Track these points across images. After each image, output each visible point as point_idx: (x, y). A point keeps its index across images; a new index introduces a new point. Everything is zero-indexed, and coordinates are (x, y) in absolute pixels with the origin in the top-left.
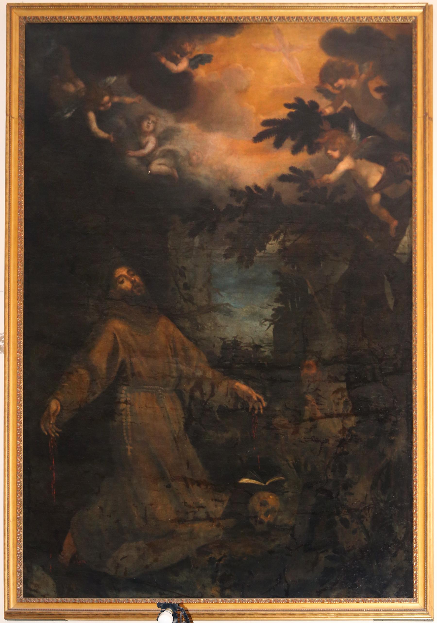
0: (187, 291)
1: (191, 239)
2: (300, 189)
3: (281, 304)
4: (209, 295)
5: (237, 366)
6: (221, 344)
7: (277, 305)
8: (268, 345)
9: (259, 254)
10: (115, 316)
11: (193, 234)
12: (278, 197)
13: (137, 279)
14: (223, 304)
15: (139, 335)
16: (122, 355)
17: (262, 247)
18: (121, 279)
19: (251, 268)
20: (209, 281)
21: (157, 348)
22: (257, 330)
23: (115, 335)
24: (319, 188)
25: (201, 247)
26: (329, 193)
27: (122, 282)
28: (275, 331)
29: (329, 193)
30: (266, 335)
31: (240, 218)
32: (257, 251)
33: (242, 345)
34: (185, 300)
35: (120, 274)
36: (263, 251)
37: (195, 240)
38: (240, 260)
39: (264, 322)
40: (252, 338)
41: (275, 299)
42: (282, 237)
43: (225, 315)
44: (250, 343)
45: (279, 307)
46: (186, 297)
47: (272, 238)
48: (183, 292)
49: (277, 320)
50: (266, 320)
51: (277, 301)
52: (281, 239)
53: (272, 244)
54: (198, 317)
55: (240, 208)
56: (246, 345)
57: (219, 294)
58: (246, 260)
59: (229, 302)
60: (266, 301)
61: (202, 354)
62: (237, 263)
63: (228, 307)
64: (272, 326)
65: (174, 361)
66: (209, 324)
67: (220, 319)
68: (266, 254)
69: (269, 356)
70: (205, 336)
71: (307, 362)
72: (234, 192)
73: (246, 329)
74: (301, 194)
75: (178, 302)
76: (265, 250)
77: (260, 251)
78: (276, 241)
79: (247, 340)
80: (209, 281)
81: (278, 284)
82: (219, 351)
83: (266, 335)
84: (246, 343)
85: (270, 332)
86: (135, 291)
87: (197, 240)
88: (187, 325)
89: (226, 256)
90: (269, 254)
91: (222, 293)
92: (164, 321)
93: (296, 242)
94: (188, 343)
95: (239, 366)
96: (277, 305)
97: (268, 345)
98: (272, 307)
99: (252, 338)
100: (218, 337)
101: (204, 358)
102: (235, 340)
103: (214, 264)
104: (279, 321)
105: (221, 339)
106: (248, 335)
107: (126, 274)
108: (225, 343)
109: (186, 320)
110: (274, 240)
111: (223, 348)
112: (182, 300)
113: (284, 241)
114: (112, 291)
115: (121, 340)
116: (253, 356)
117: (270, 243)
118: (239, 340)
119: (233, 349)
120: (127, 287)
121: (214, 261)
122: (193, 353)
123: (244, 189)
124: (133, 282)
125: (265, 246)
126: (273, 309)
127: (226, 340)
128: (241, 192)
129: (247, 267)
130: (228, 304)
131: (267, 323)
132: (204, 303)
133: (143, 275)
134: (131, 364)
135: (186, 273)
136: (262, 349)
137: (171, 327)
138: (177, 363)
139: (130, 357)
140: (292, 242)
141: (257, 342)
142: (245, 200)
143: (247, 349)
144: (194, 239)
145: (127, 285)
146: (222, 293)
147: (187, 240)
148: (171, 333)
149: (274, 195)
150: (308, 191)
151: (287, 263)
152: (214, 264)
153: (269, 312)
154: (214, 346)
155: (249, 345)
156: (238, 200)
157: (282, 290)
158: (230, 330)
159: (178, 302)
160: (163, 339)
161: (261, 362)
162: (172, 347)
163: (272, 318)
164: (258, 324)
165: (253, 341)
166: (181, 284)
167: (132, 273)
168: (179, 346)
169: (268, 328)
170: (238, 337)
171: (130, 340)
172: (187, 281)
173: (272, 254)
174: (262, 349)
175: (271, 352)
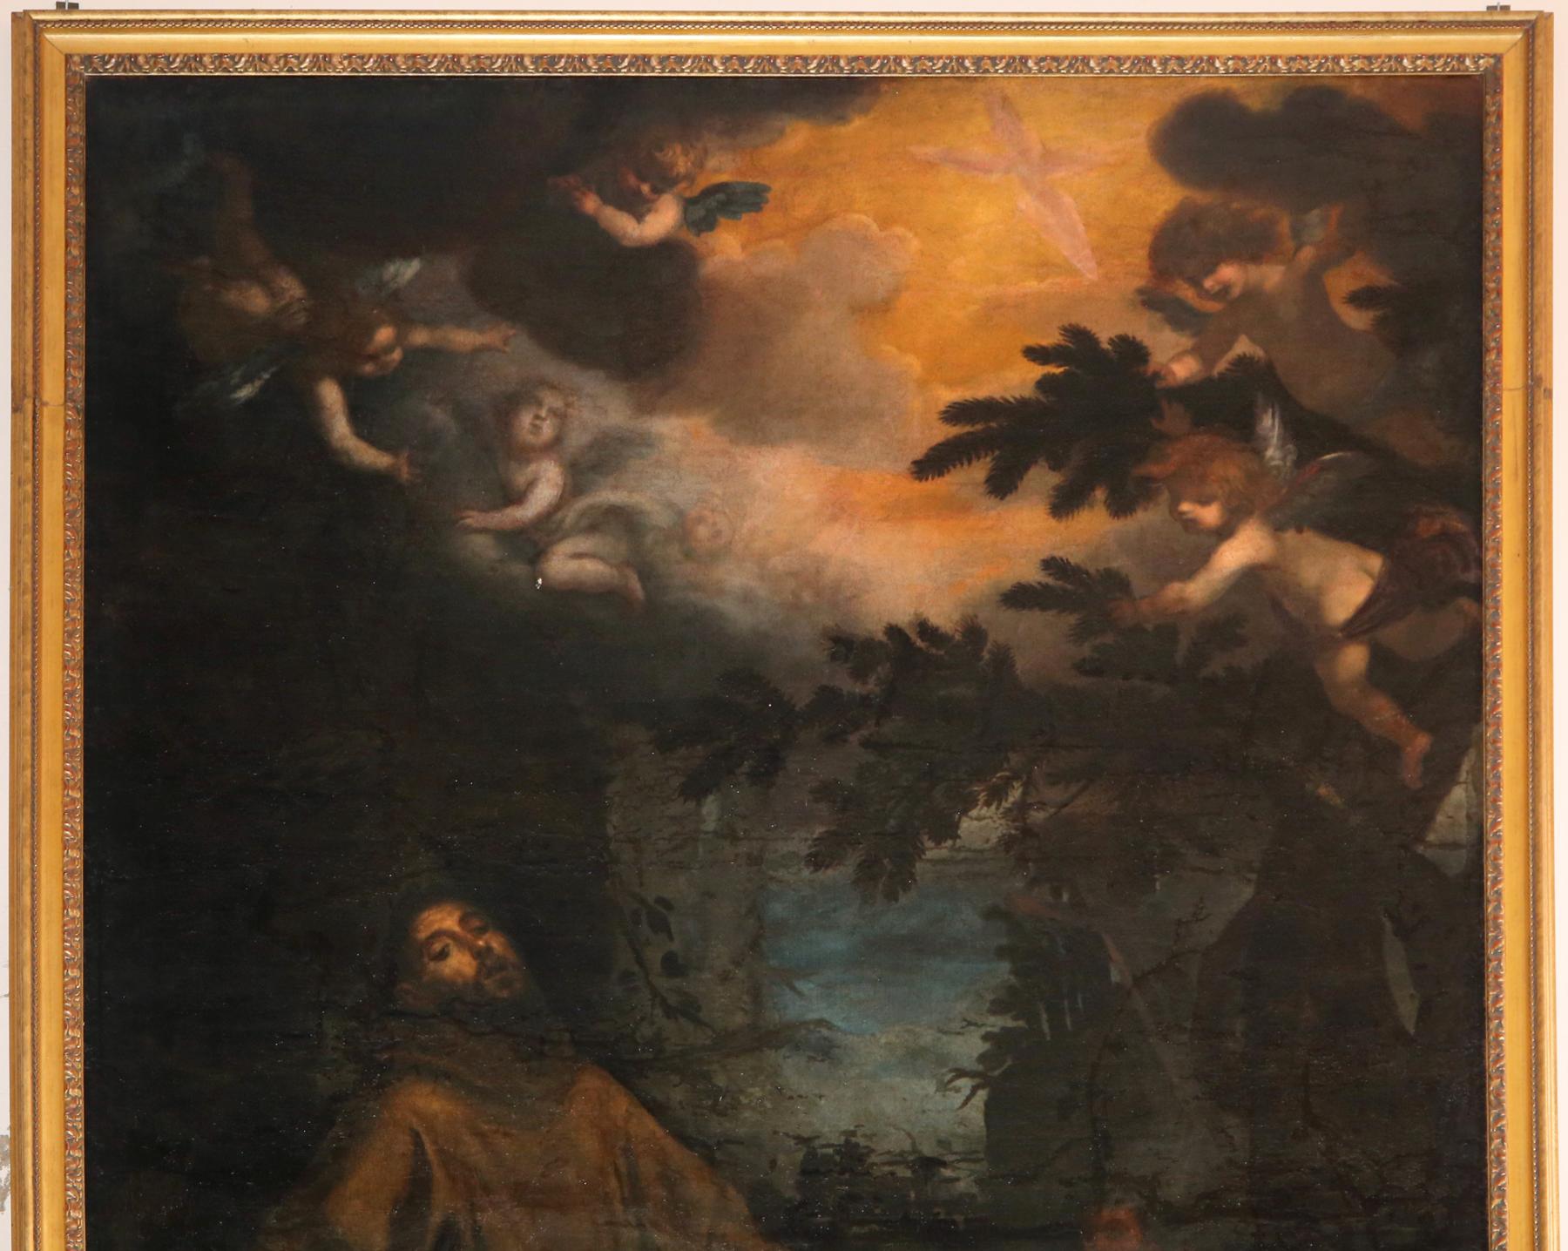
0: (677, 982)
1: (691, 805)
2: (1080, 633)
3: (1015, 1018)
4: (756, 995)
5: (855, 1229)
6: (800, 1156)
7: (997, 1023)
8: (968, 1157)
9: (933, 852)
10: (417, 1070)
11: (695, 789)
12: (1003, 659)
13: (495, 942)
14: (805, 1024)
15: (506, 1134)
16: (443, 1205)
17: (946, 829)
18: (437, 947)
19: (903, 900)
20: (754, 945)
21: (569, 1175)
22: (929, 1106)
23: (417, 1135)
24: (1149, 627)
25: (728, 834)
26: (1184, 643)
27: (443, 955)
28: (990, 1108)
29: (1184, 643)
30: (961, 1123)
31: (865, 732)
32: (929, 844)
33: (873, 1159)
34: (670, 1012)
35: (436, 927)
36: (949, 843)
37: (704, 811)
38: (867, 873)
39: (950, 1081)
40: (909, 1135)
41: (993, 1002)
42: (1015, 794)
43: (811, 1058)
44: (902, 1153)
45: (1003, 1028)
46: (673, 1000)
47: (982, 797)
48: (663, 983)
49: (996, 1073)
50: (961, 1073)
51: (998, 1007)
52: (1011, 799)
53: (979, 819)
54: (715, 1067)
55: (865, 700)
56: (885, 1158)
57: (793, 988)
58: (888, 869)
59: (826, 1015)
60: (961, 1007)
61: (732, 1192)
62: (856, 882)
63: (825, 1032)
64: (982, 1094)
65: (631, 1219)
66: (756, 1091)
67: (793, 1071)
68: (959, 850)
69: (973, 1196)
70: (741, 1131)
71: (1106, 1213)
72: (846, 646)
73: (889, 1107)
74: (1086, 650)
75: (643, 1019)
76: (956, 837)
77: (938, 842)
78: (993, 807)
79: (894, 1142)
80: (754, 945)
81: (1001, 953)
82: (791, 1182)
83: (961, 1123)
84: (889, 1152)
85: (975, 1114)
86: (489, 984)
87: (710, 807)
88: (677, 1095)
89: (817, 861)
90: (969, 850)
91: (801, 985)
92: (592, 1082)
93: (1065, 811)
94: (681, 1158)
95: (865, 1230)
96: (997, 1023)
97: (968, 1157)
98: (983, 1031)
99: (909, 1135)
100: (787, 1135)
101: (739, 1205)
102: (847, 1142)
103: (774, 887)
104: (1008, 1078)
105: (800, 1140)
106: (894, 1126)
107: (457, 929)
108: (811, 1154)
109: (675, 1079)
110: (988, 804)
111: (804, 1172)
112: (658, 1011)
113: (1022, 807)
114: (405, 986)
115: (440, 1151)
116: (913, 1195)
117: (974, 813)
118: (862, 1142)
119: (842, 1173)
120: (458, 972)
121: (772, 878)
122: (700, 1190)
123: (881, 637)
124: (480, 955)
125: (957, 826)
126: (985, 1038)
127: (817, 1143)
128: (869, 644)
129: (891, 896)
130: (821, 1022)
131: (965, 1084)
132: (739, 1019)
133: (515, 930)
134: (476, 1230)
135: (673, 920)
136: (947, 1173)
137: (621, 1105)
138: (640, 1225)
139: (473, 1209)
140: (1052, 810)
141: (928, 1150)
142: (883, 670)
143: (893, 1174)
144: (699, 805)
145: (459, 963)
146: (801, 985)
147: (676, 808)
148: (620, 1123)
149: (986, 655)
150: (1109, 639)
151: (1033, 882)
152: (774, 887)
153: (969, 1048)
154: (773, 1163)
155: (899, 1159)
156: (859, 674)
157: (1015, 972)
158: (829, 1109)
159: (643, 1019)
160: (589, 1145)
161: (942, 1217)
162: (623, 1170)
163: (981, 1068)
164: (930, 1087)
165: (914, 1144)
166: (654, 956)
167: (476, 923)
168: (648, 1167)
169: (968, 1099)
170: (859, 1133)
171: (472, 1149)
172: (675, 946)
173: (982, 851)
174: (947, 1173)
175: (979, 1182)
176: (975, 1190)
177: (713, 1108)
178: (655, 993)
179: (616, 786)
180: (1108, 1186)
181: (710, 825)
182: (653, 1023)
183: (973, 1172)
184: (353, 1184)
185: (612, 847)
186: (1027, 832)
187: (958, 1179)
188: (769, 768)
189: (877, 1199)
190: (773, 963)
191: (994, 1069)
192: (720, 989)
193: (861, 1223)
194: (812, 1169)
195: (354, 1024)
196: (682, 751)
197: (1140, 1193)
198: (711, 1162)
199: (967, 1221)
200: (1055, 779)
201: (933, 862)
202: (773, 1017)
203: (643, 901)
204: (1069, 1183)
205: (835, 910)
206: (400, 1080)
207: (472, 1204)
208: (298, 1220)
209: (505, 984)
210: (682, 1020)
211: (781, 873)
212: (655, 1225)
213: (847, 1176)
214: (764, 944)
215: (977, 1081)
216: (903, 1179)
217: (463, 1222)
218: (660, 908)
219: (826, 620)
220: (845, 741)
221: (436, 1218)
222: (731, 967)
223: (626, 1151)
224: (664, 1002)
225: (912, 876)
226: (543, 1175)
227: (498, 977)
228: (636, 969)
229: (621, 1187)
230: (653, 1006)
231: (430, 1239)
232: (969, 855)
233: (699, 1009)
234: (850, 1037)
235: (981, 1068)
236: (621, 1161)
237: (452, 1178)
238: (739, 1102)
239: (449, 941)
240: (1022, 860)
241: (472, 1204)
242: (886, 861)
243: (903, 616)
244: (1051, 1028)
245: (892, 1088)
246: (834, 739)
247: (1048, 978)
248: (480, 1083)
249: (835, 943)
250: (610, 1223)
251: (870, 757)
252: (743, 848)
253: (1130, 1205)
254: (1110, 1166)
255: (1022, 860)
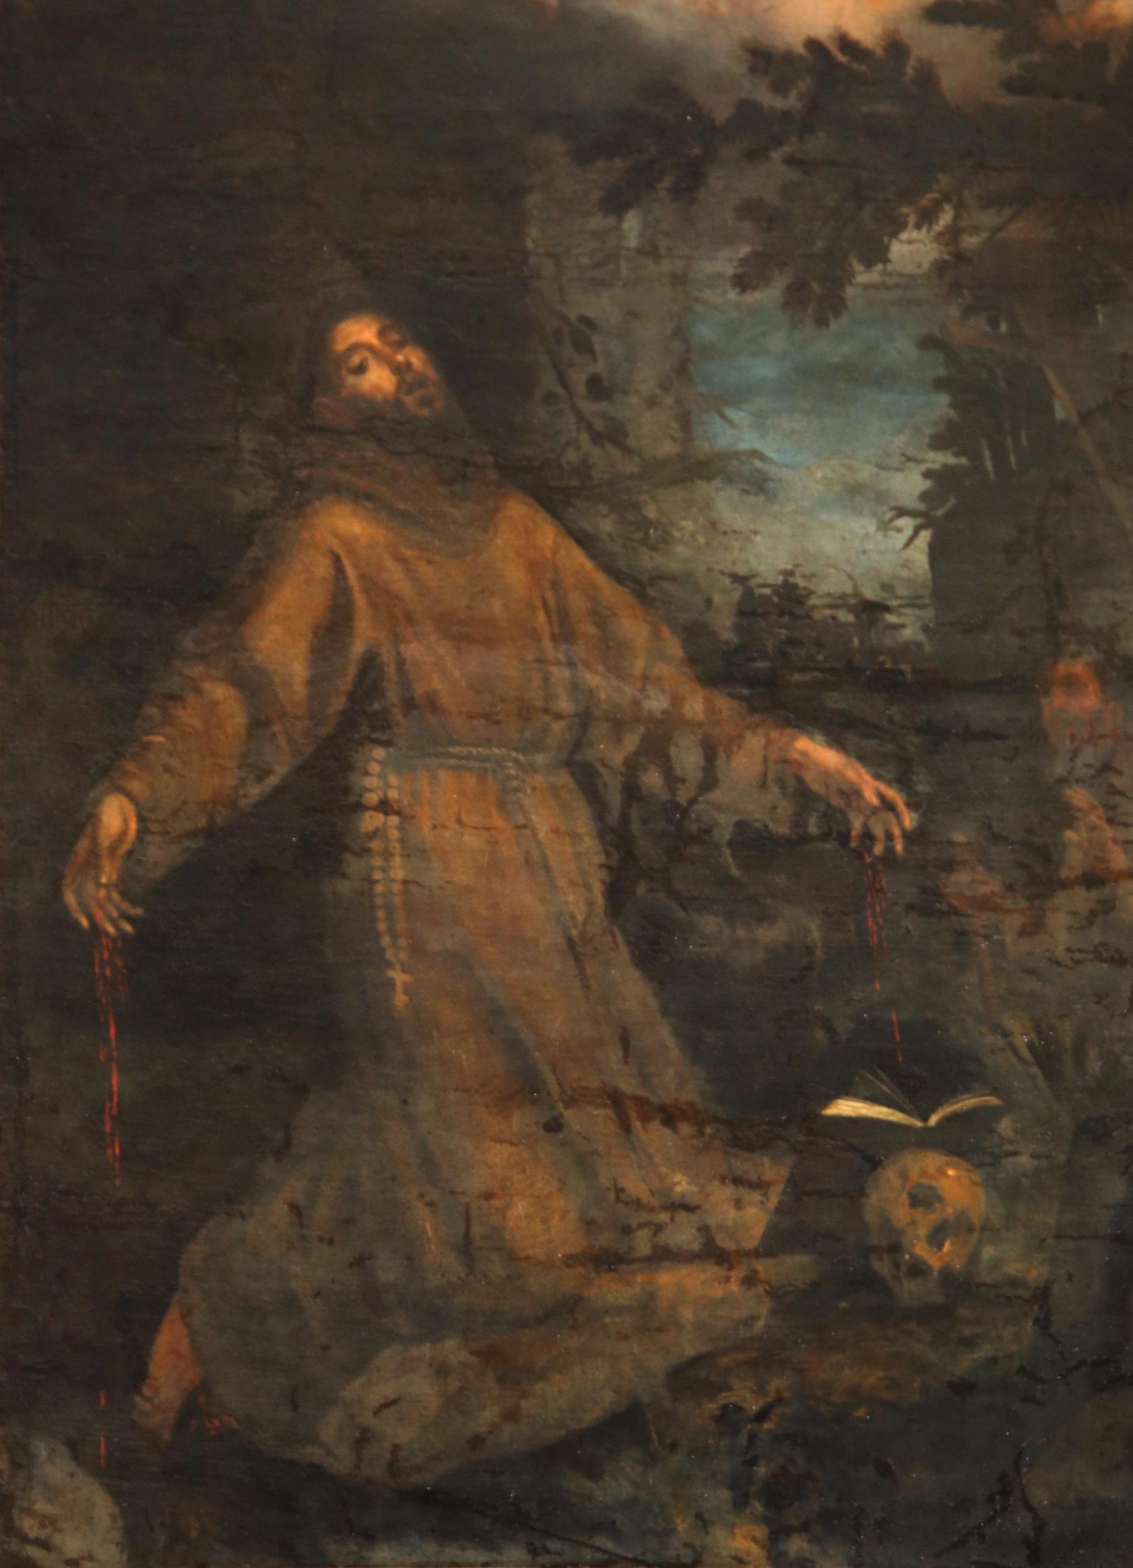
0: (602, 406)
1: (611, 220)
2: (1006, 50)
3: (957, 455)
4: (685, 421)
5: (797, 677)
6: (737, 595)
7: (938, 459)
8: (913, 602)
9: (864, 276)
10: (337, 490)
11: (616, 203)
12: (927, 78)
13: (415, 357)
14: (737, 455)
15: (429, 562)
16: (366, 631)
17: (876, 254)
18: (356, 360)
19: (835, 325)
20: (681, 370)
21: (496, 607)
22: (870, 546)
23: (337, 559)
24: (1078, 45)
25: (650, 251)
26: (1114, 62)
27: (361, 369)
28: (935, 552)
29: (1114, 62)
30: (904, 566)
31: (787, 149)
32: (859, 267)
33: (813, 601)
34: (597, 438)
35: (354, 339)
36: (879, 267)
37: (626, 225)
38: (796, 297)
39: (892, 520)
40: (850, 577)
41: (932, 437)
42: (946, 217)
43: (745, 492)
44: (843, 596)
45: (946, 466)
46: (599, 425)
47: (912, 219)
48: (589, 407)
49: (940, 512)
50: (902, 512)
51: (939, 442)
52: (942, 222)
53: (910, 242)
54: (646, 497)
55: (785, 116)
56: (827, 601)
57: (723, 416)
58: (817, 296)
59: (759, 446)
60: (899, 442)
61: (666, 632)
62: (785, 305)
63: (758, 464)
64: (925, 536)
65: (562, 657)
66: (688, 525)
67: (727, 504)
68: (890, 275)
69: (919, 645)
70: (674, 566)
71: (1063, 667)
72: (763, 58)
73: (828, 546)
74: (1013, 67)
75: (568, 444)
76: (886, 261)
77: (869, 264)
78: (924, 230)
79: (832, 584)
80: (681, 370)
81: (940, 384)
82: (728, 623)
83: (904, 566)
84: (829, 595)
85: (919, 556)
86: (409, 401)
87: (632, 223)
88: (606, 526)
89: (742, 283)
90: (902, 275)
91: (730, 412)
92: (518, 509)
93: (1001, 235)
94: (610, 591)
95: (808, 677)
96: (938, 459)
97: (913, 602)
98: (923, 467)
99: (850, 577)
100: (722, 572)
101: (674, 647)
102: (786, 582)
103: (699, 308)
104: (954, 517)
105: (736, 578)
106: (835, 567)
107: (375, 341)
108: (748, 594)
109: (603, 508)
110: (918, 227)
111: (741, 613)
112: (584, 436)
113: (953, 234)
114: (324, 400)
115: (362, 577)
116: (856, 641)
117: (904, 236)
118: (801, 583)
119: (782, 614)
120: (378, 388)
121: (697, 300)
122: (633, 628)
123: (800, 49)
124: (399, 370)
125: (886, 249)
126: (927, 474)
127: (753, 582)
128: (788, 58)
129: (822, 322)
130: (755, 454)
131: (907, 524)
132: (668, 448)
133: (433, 345)
134: (401, 664)
135: (596, 339)
136: (892, 619)
137: (548, 534)
138: (571, 664)
139: (397, 639)
140: (985, 235)
141: (871, 593)
142: (804, 84)
143: (834, 618)
144: (620, 219)
145: (378, 379)
146: (730, 412)
147: (597, 222)
148: (548, 554)
149: (910, 71)
150: (1036, 57)
151: (968, 311)
152: (699, 308)
153: (910, 485)
154: (709, 602)
155: (839, 602)
156: (780, 87)
157: (954, 405)
159: (568, 444)
160: (516, 576)
161: (888, 666)
162: (552, 604)
163: (922, 507)
164: (871, 526)
165: (855, 587)
166: (578, 379)
167: (395, 336)
168: (577, 603)
169: (911, 540)
170: (798, 572)
171: (395, 576)
172: (600, 368)
173: (913, 277)
174: (892, 619)
175: (926, 629)
176: (921, 637)
177: (644, 542)
178: (580, 417)
179: (532, 200)
180: (1063, 637)
181: (633, 242)
182: (578, 448)
183: (919, 618)
184: (273, 608)
185: (532, 260)
186: (960, 258)
187: (903, 626)
188: (690, 182)
189: (820, 645)
190: (702, 388)
191: (936, 508)
192: (647, 414)
193: (803, 670)
194: (751, 609)
195: (272, 438)
196: (600, 164)
197: (1096, 646)
198: (643, 598)
199: (915, 671)
200: (987, 203)
201: (867, 287)
202: (702, 447)
203: (564, 319)
204: (1021, 634)
205: (764, 335)
206: (320, 499)
207: (395, 635)
208: (216, 645)
209: (426, 402)
210: (609, 447)
211: (707, 294)
212: (587, 665)
213: (786, 619)
214: (691, 368)
215: (919, 521)
216: (846, 624)
217: (386, 654)
218: (583, 327)
219: (745, 31)
220: (768, 158)
221: (358, 649)
222: (658, 391)
223: (555, 585)
224: (590, 427)
225: (842, 300)
226: (469, 607)
227: (418, 394)
228: (560, 390)
229: (550, 622)
230: (579, 431)
231: (352, 671)
232: (901, 280)
233: (626, 435)
234: (785, 470)
235: (922, 507)
236: (549, 595)
237: (373, 605)
238: (671, 535)
239: (368, 354)
240: (956, 288)
241: (395, 635)
242: (814, 285)
243: (821, 27)
244: (994, 466)
245: (830, 526)
246: (756, 155)
247: (985, 407)
248: (402, 506)
249: (765, 370)
250: (539, 661)
251: (793, 175)
252: (666, 266)
253: (1087, 658)
254: (1063, 617)
255: (956, 288)
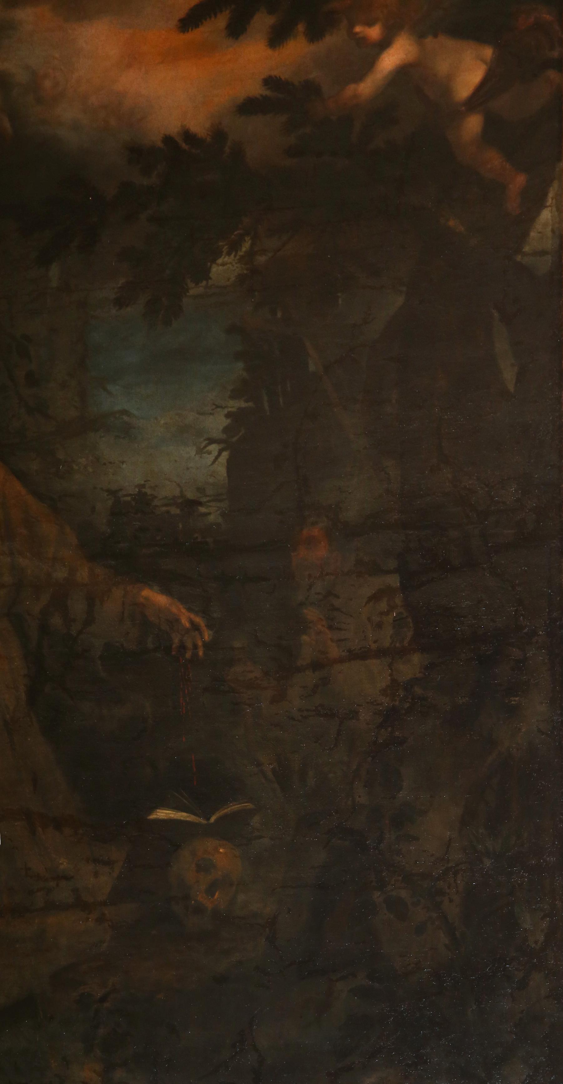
3: (246, 401)
6: (110, 503)
7: (235, 405)
9: (194, 290)
17: (202, 274)
32: (191, 285)
33: (156, 502)
36: (204, 283)
39: (205, 447)
42: (246, 246)
45: (239, 409)
47: (225, 249)
49: (235, 439)
50: (211, 441)
51: (235, 395)
52: (244, 249)
53: (223, 264)
63: (126, 418)
64: (225, 454)
66: (83, 461)
76: (208, 278)
84: (166, 497)
85: (221, 469)
87: (54, 271)
89: (120, 302)
91: (110, 387)
96: (235, 405)
98: (226, 411)
99: (179, 485)
100: (102, 489)
102: (140, 492)
104: (243, 441)
105: (113, 493)
110: (229, 254)
117: (220, 261)
118: (149, 491)
125: (208, 271)
126: (228, 416)
130: (125, 412)
131: (214, 448)
136: (202, 510)
141: (190, 495)
143: (168, 512)
146: (110, 387)
153: (217, 423)
158: (129, 471)
163: (224, 436)
164: (192, 451)
165: (181, 491)
169: (216, 458)
174: (202, 510)
187: (209, 514)
215: (222, 446)
235: (224, 436)
